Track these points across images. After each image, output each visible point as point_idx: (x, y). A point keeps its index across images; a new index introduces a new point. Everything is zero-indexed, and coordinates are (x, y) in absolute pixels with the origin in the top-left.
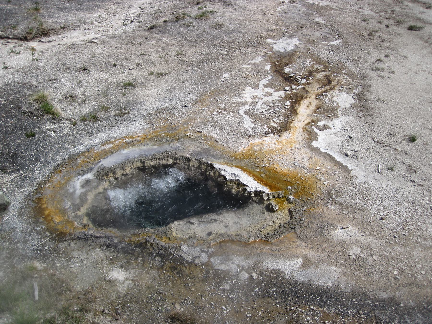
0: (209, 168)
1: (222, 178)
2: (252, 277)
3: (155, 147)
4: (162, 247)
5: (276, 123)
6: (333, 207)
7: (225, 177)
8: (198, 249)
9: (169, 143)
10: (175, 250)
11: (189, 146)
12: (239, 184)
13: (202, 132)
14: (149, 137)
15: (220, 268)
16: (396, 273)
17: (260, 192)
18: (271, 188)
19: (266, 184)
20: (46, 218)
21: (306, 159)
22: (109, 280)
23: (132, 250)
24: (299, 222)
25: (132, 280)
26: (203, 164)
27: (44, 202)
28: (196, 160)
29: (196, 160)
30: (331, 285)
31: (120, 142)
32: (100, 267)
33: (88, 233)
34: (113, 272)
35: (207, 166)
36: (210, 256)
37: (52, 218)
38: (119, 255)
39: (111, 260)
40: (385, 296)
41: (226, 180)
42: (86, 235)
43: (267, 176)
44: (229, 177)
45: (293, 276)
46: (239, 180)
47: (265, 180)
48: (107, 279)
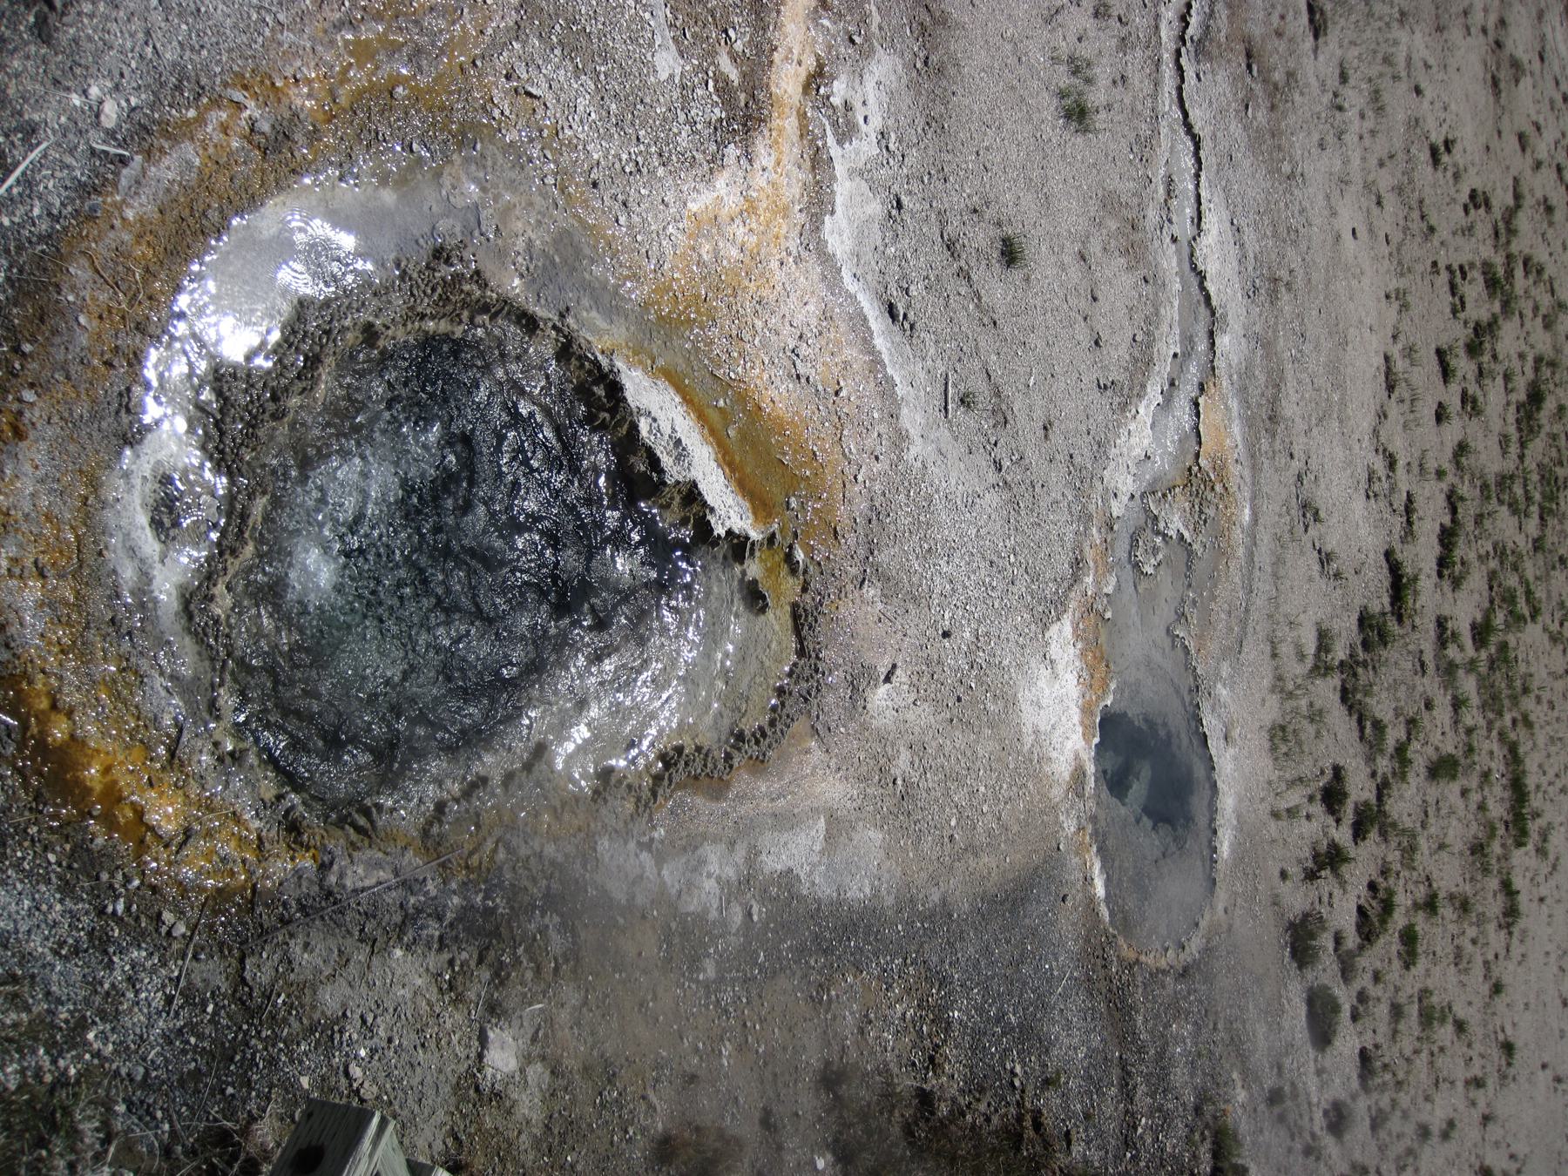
0: (600, 391)
1: (643, 452)
2: (750, 915)
3: (388, 197)
4: (553, 863)
5: (734, 57)
6: (872, 592)
7: (654, 462)
8: (632, 845)
9: (438, 174)
10: (584, 866)
11: (510, 208)
12: (692, 495)
13: (538, 98)
14: (343, 101)
15: (692, 908)
16: (953, 823)
17: (739, 536)
18: (761, 506)
19: (744, 485)
20: (109, 820)
21: (814, 322)
22: (496, 1095)
23: (489, 912)
24: (817, 671)
25: (543, 1058)
26: (580, 358)
27: (44, 704)
28: (554, 327)
29: (554, 327)
30: (867, 890)
31: (225, 129)
32: (438, 1041)
33: (344, 887)
34: (492, 1052)
35: (590, 372)
36: (660, 860)
37: (139, 813)
38: (464, 955)
39: (451, 988)
40: (936, 897)
41: (665, 484)
42: (330, 893)
43: (744, 436)
44: (673, 471)
45: (813, 884)
46: (694, 484)
47: (737, 458)
48: (486, 1086)
